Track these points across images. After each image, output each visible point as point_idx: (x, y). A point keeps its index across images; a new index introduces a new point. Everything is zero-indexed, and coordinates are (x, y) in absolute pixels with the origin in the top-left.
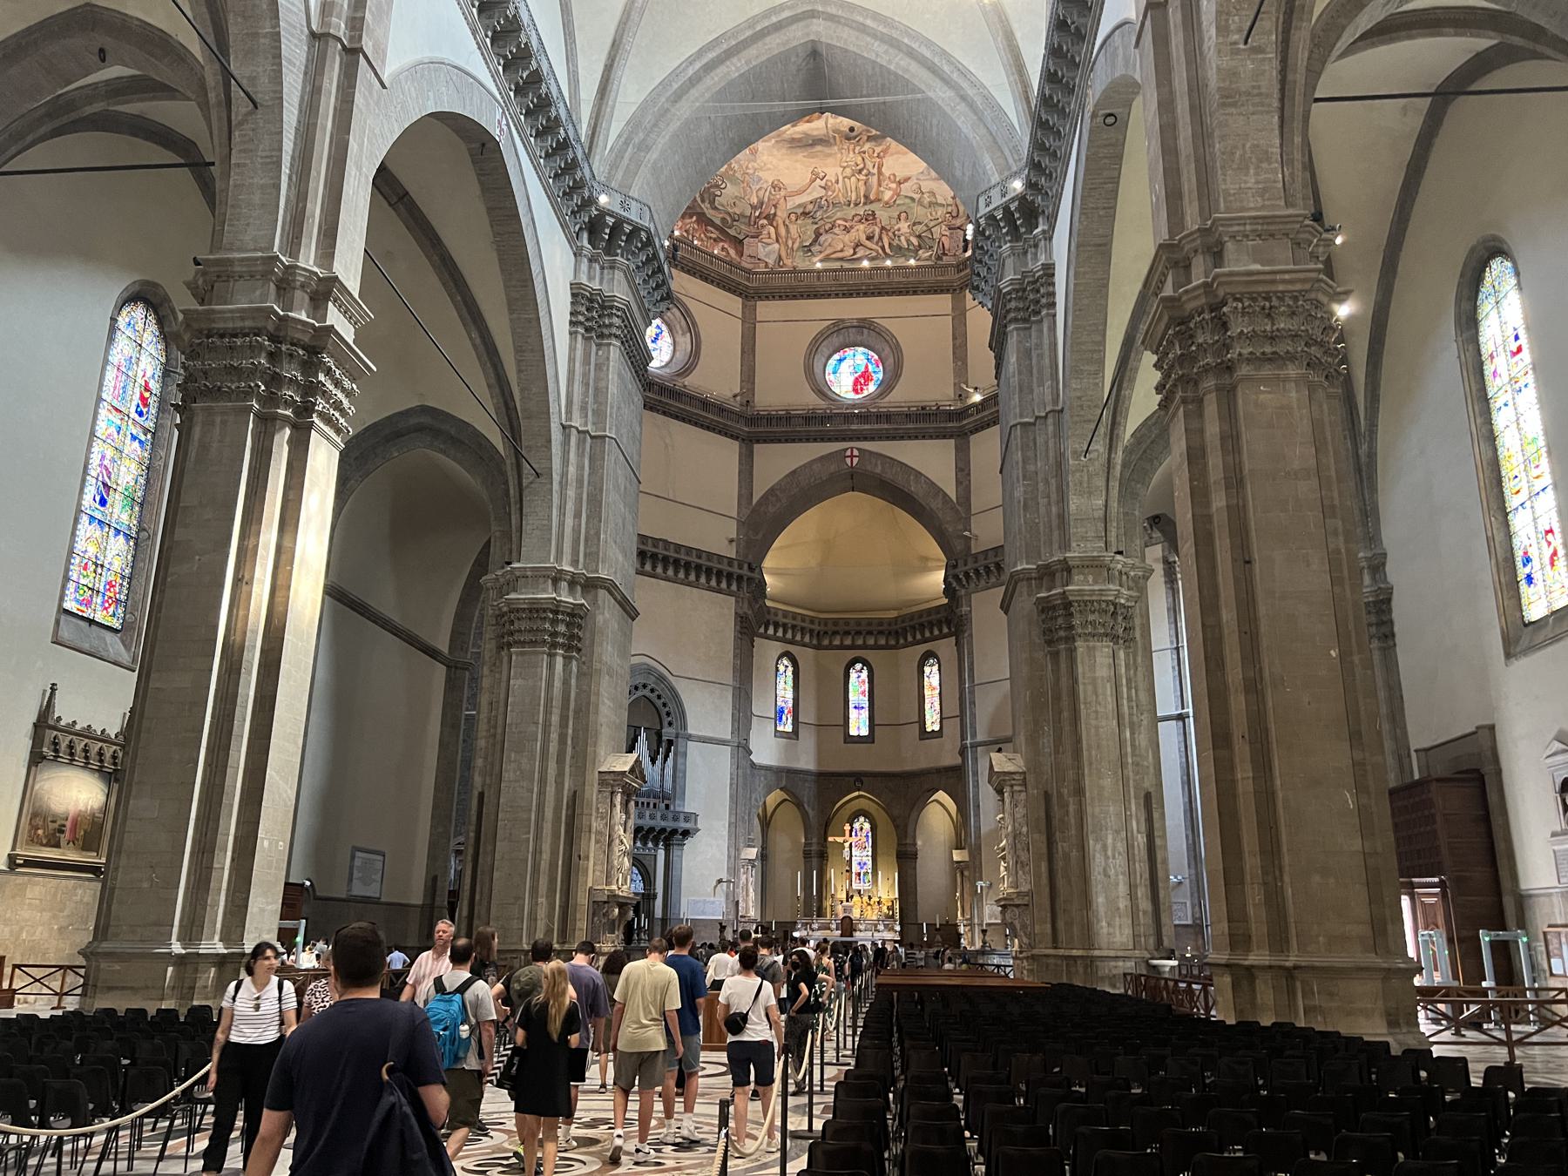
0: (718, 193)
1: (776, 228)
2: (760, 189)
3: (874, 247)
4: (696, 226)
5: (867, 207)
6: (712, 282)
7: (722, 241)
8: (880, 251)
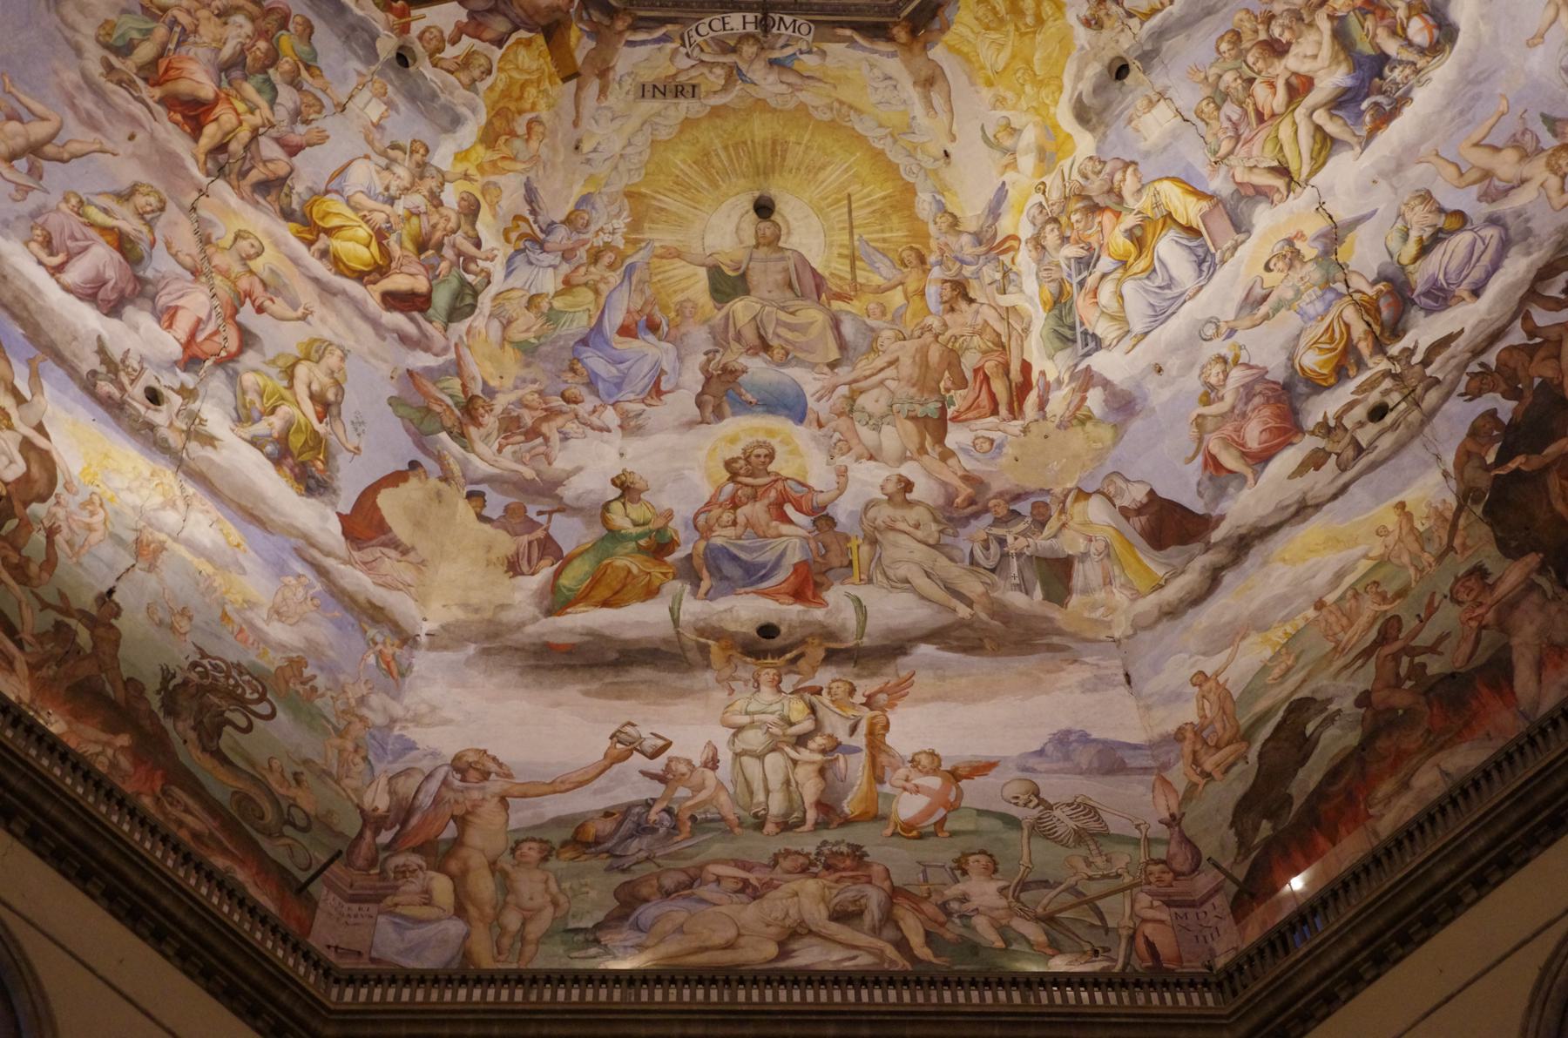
0: (243, 723)
1: (459, 881)
2: (407, 772)
3: (863, 939)
4: (125, 762)
5: (831, 835)
6: (157, 937)
7: (225, 852)
8: (891, 952)
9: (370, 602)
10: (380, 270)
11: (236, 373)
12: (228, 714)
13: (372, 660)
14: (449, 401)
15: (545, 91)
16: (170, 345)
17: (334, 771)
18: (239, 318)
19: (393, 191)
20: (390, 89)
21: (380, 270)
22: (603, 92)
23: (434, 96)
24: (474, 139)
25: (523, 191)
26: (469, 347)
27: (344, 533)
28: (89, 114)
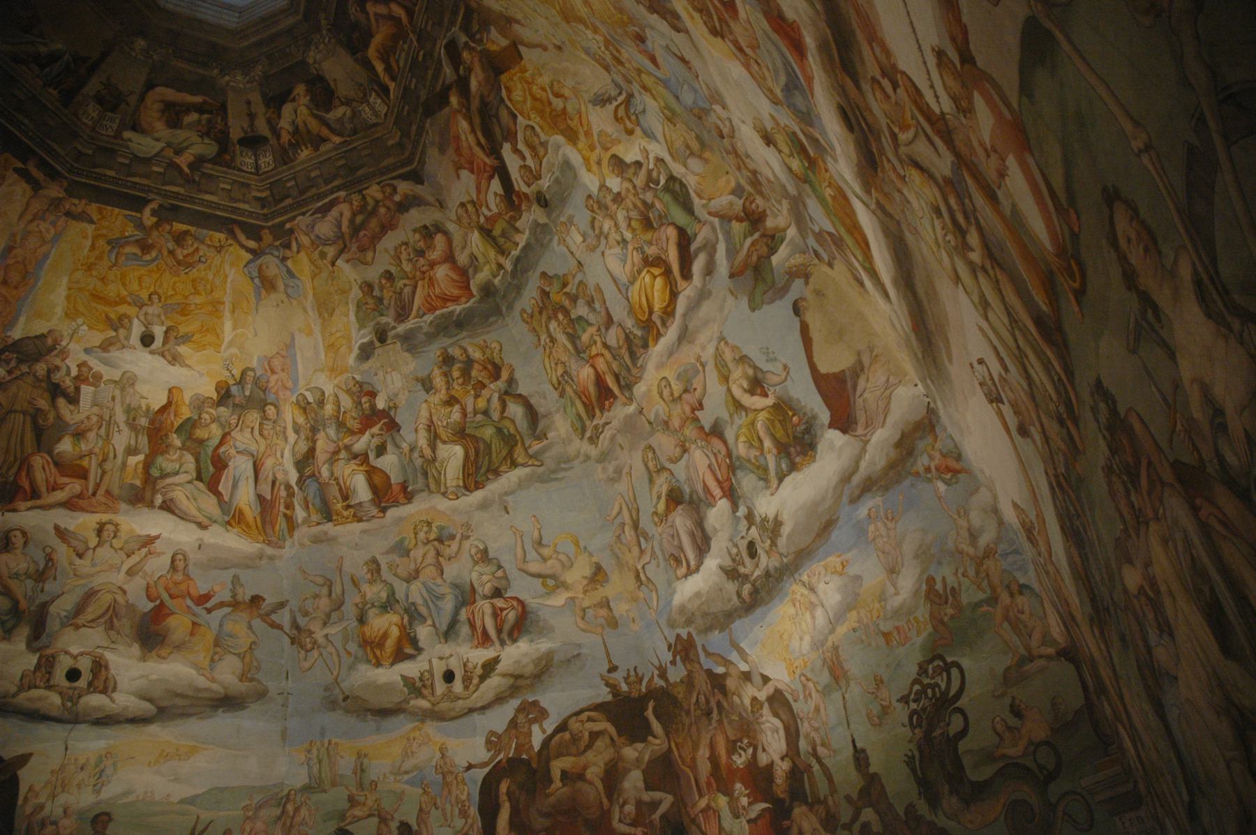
9: (899, 444)
10: (668, 273)
11: (738, 458)
12: (952, 730)
13: (942, 487)
14: (749, 241)
15: (533, 76)
16: (723, 504)
17: (1022, 651)
18: (707, 429)
19: (619, 239)
20: (563, 219)
21: (668, 273)
22: (518, 22)
23: (557, 181)
24: (575, 151)
25: (598, 108)
26: (710, 200)
27: (844, 431)
28: (615, 472)
